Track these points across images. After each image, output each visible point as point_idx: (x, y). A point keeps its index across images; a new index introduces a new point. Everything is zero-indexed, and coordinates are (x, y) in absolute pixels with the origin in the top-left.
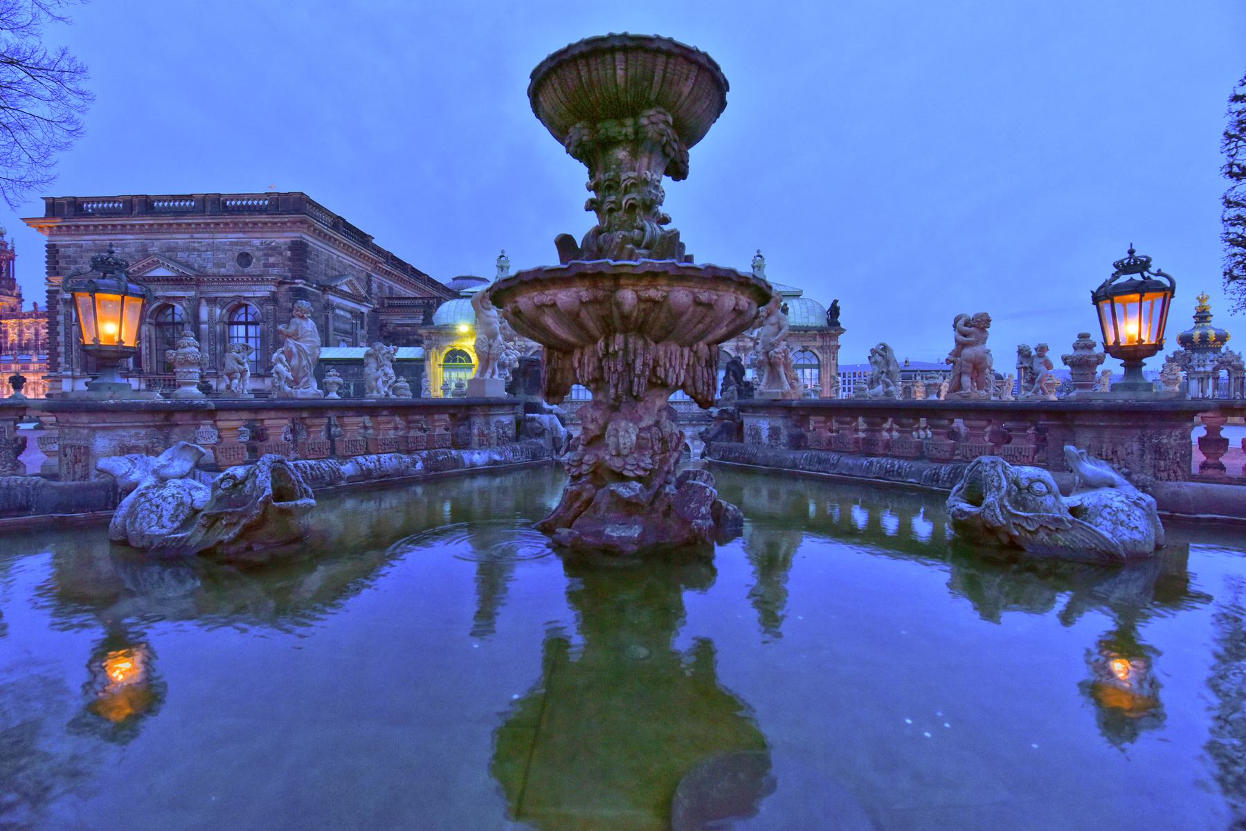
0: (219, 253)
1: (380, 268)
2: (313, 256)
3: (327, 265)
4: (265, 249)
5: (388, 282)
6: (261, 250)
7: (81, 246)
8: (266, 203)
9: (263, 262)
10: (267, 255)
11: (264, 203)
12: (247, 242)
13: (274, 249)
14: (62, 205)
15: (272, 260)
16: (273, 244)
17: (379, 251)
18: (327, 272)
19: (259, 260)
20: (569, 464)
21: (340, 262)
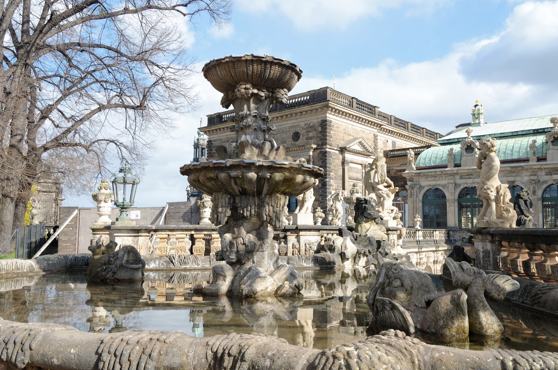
0: (283, 134)
1: (384, 129)
2: (334, 129)
3: (345, 133)
4: (307, 128)
5: (391, 139)
6: (305, 129)
7: (222, 140)
8: (308, 98)
9: (306, 136)
10: (308, 132)
11: (307, 98)
12: (297, 126)
13: (310, 127)
14: (214, 118)
15: (311, 134)
16: (311, 124)
17: (384, 116)
18: (345, 138)
19: (303, 136)
20: (233, 238)
21: (353, 129)
